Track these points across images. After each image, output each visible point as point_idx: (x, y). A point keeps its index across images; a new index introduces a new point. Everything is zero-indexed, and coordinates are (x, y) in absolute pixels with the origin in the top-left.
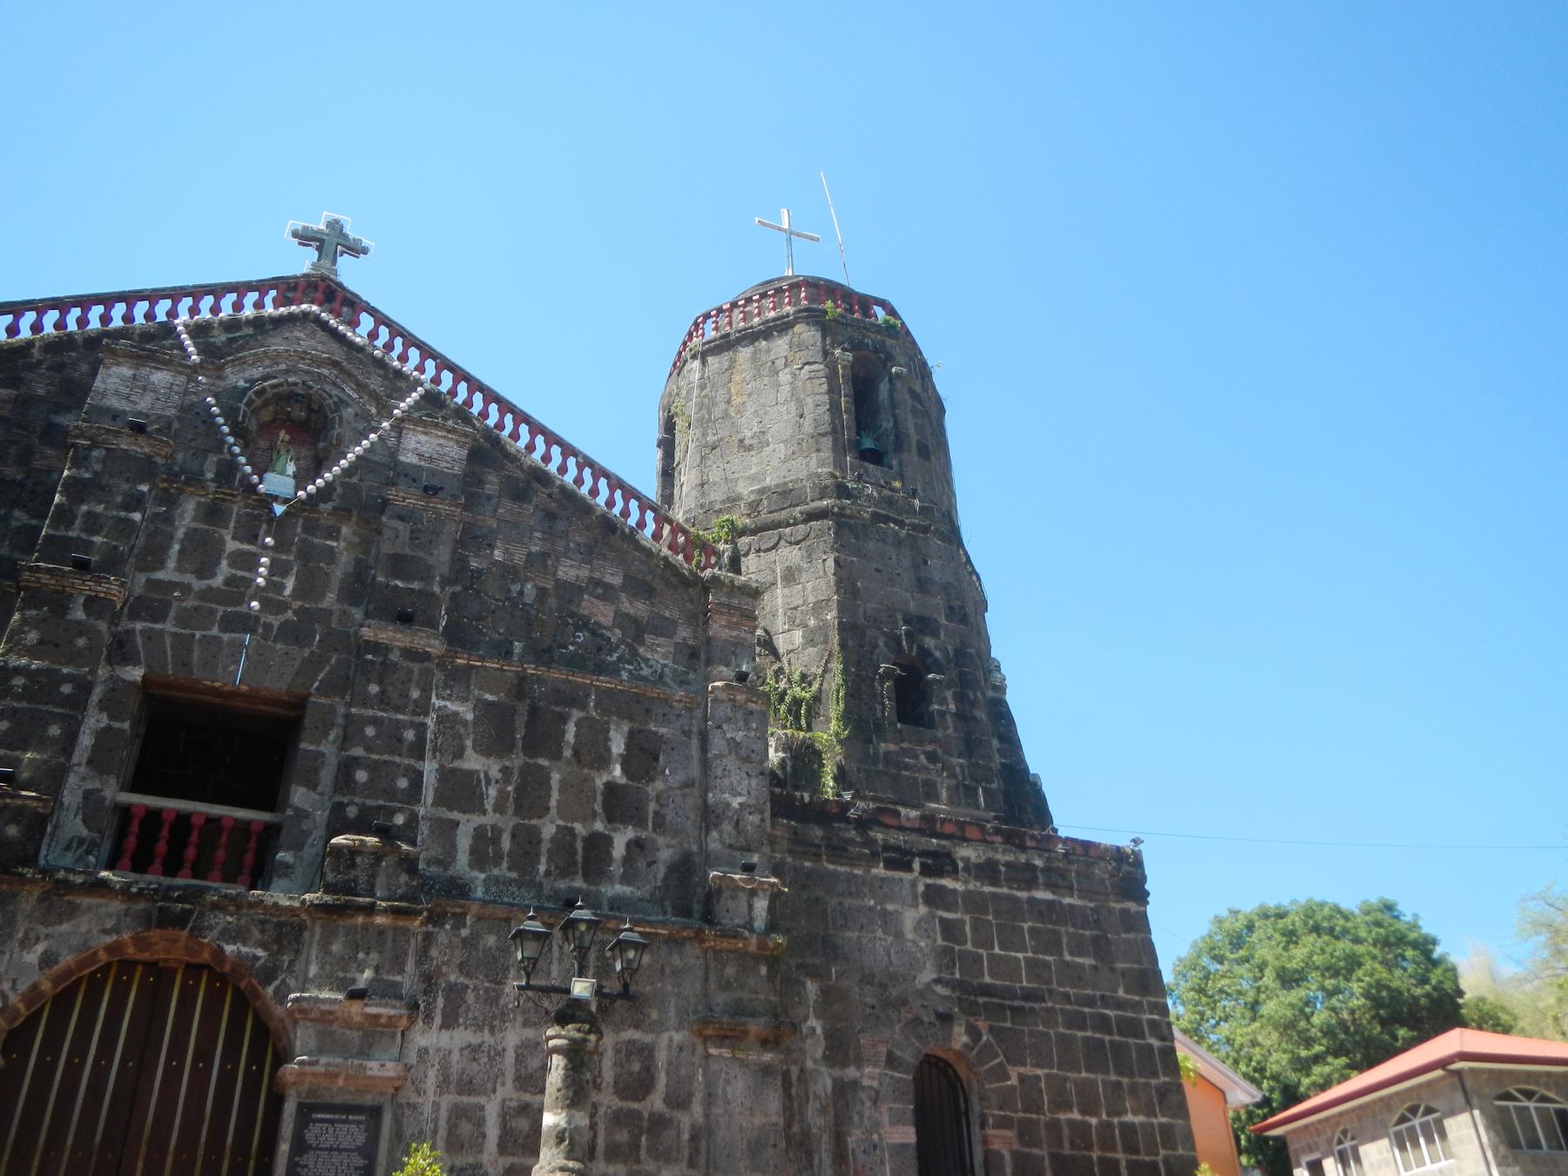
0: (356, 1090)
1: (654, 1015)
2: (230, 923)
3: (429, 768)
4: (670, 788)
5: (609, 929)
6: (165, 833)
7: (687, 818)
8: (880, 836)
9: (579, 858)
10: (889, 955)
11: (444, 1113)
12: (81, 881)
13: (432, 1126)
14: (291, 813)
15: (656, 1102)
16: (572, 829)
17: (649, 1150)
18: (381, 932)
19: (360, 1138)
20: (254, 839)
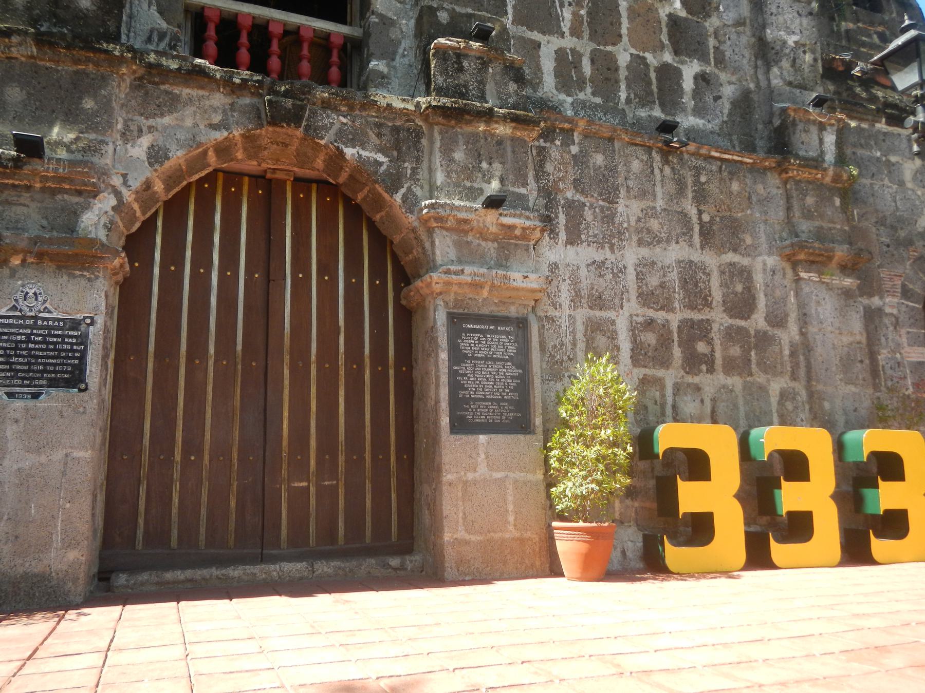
0: (501, 302)
1: (749, 240)
2: (345, 124)
4: (725, 25)
5: (701, 155)
6: (244, 39)
7: (743, 56)
8: (880, 94)
9: (654, 88)
10: (895, 202)
11: (580, 328)
12: (176, 66)
13: (571, 338)
14: (377, 20)
15: (758, 321)
16: (644, 58)
17: (758, 364)
18: (500, 143)
19: (512, 350)
20: (335, 53)
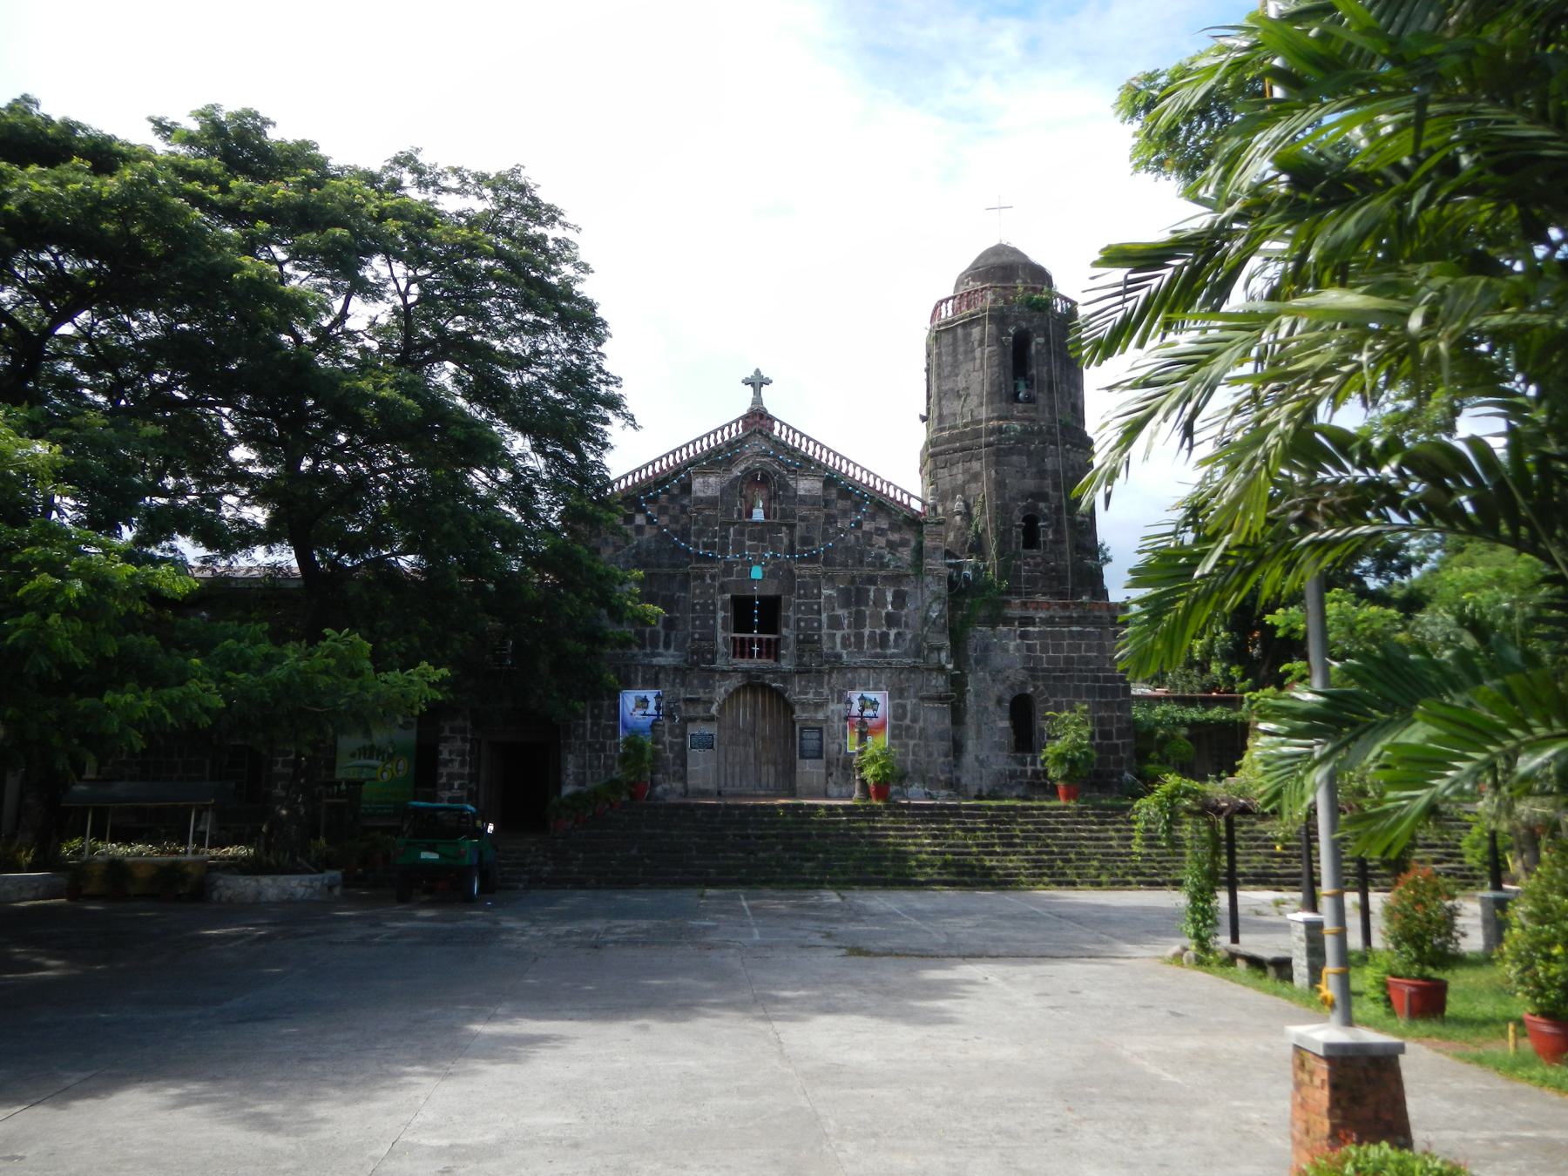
3: (824, 616)
15: (907, 722)
